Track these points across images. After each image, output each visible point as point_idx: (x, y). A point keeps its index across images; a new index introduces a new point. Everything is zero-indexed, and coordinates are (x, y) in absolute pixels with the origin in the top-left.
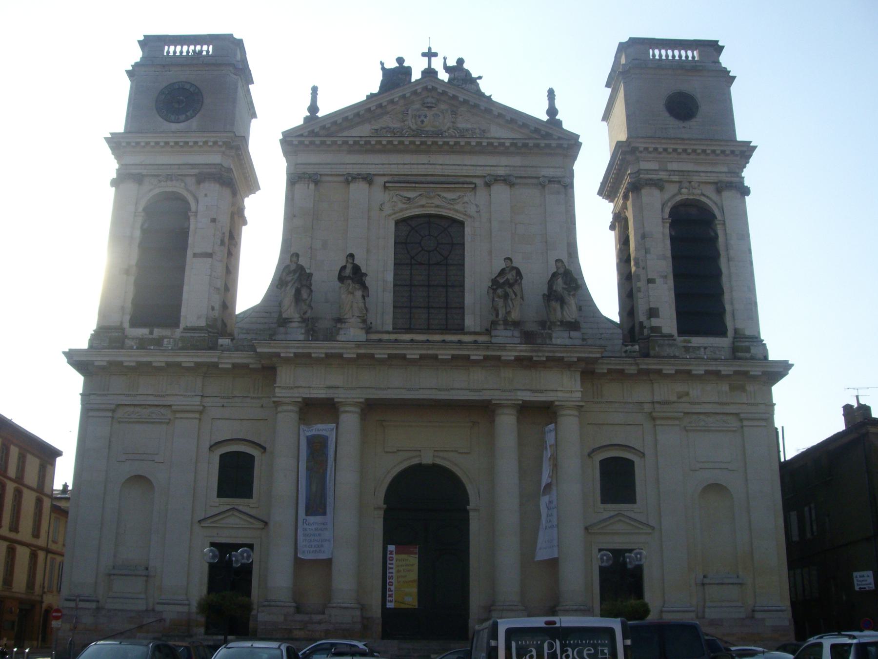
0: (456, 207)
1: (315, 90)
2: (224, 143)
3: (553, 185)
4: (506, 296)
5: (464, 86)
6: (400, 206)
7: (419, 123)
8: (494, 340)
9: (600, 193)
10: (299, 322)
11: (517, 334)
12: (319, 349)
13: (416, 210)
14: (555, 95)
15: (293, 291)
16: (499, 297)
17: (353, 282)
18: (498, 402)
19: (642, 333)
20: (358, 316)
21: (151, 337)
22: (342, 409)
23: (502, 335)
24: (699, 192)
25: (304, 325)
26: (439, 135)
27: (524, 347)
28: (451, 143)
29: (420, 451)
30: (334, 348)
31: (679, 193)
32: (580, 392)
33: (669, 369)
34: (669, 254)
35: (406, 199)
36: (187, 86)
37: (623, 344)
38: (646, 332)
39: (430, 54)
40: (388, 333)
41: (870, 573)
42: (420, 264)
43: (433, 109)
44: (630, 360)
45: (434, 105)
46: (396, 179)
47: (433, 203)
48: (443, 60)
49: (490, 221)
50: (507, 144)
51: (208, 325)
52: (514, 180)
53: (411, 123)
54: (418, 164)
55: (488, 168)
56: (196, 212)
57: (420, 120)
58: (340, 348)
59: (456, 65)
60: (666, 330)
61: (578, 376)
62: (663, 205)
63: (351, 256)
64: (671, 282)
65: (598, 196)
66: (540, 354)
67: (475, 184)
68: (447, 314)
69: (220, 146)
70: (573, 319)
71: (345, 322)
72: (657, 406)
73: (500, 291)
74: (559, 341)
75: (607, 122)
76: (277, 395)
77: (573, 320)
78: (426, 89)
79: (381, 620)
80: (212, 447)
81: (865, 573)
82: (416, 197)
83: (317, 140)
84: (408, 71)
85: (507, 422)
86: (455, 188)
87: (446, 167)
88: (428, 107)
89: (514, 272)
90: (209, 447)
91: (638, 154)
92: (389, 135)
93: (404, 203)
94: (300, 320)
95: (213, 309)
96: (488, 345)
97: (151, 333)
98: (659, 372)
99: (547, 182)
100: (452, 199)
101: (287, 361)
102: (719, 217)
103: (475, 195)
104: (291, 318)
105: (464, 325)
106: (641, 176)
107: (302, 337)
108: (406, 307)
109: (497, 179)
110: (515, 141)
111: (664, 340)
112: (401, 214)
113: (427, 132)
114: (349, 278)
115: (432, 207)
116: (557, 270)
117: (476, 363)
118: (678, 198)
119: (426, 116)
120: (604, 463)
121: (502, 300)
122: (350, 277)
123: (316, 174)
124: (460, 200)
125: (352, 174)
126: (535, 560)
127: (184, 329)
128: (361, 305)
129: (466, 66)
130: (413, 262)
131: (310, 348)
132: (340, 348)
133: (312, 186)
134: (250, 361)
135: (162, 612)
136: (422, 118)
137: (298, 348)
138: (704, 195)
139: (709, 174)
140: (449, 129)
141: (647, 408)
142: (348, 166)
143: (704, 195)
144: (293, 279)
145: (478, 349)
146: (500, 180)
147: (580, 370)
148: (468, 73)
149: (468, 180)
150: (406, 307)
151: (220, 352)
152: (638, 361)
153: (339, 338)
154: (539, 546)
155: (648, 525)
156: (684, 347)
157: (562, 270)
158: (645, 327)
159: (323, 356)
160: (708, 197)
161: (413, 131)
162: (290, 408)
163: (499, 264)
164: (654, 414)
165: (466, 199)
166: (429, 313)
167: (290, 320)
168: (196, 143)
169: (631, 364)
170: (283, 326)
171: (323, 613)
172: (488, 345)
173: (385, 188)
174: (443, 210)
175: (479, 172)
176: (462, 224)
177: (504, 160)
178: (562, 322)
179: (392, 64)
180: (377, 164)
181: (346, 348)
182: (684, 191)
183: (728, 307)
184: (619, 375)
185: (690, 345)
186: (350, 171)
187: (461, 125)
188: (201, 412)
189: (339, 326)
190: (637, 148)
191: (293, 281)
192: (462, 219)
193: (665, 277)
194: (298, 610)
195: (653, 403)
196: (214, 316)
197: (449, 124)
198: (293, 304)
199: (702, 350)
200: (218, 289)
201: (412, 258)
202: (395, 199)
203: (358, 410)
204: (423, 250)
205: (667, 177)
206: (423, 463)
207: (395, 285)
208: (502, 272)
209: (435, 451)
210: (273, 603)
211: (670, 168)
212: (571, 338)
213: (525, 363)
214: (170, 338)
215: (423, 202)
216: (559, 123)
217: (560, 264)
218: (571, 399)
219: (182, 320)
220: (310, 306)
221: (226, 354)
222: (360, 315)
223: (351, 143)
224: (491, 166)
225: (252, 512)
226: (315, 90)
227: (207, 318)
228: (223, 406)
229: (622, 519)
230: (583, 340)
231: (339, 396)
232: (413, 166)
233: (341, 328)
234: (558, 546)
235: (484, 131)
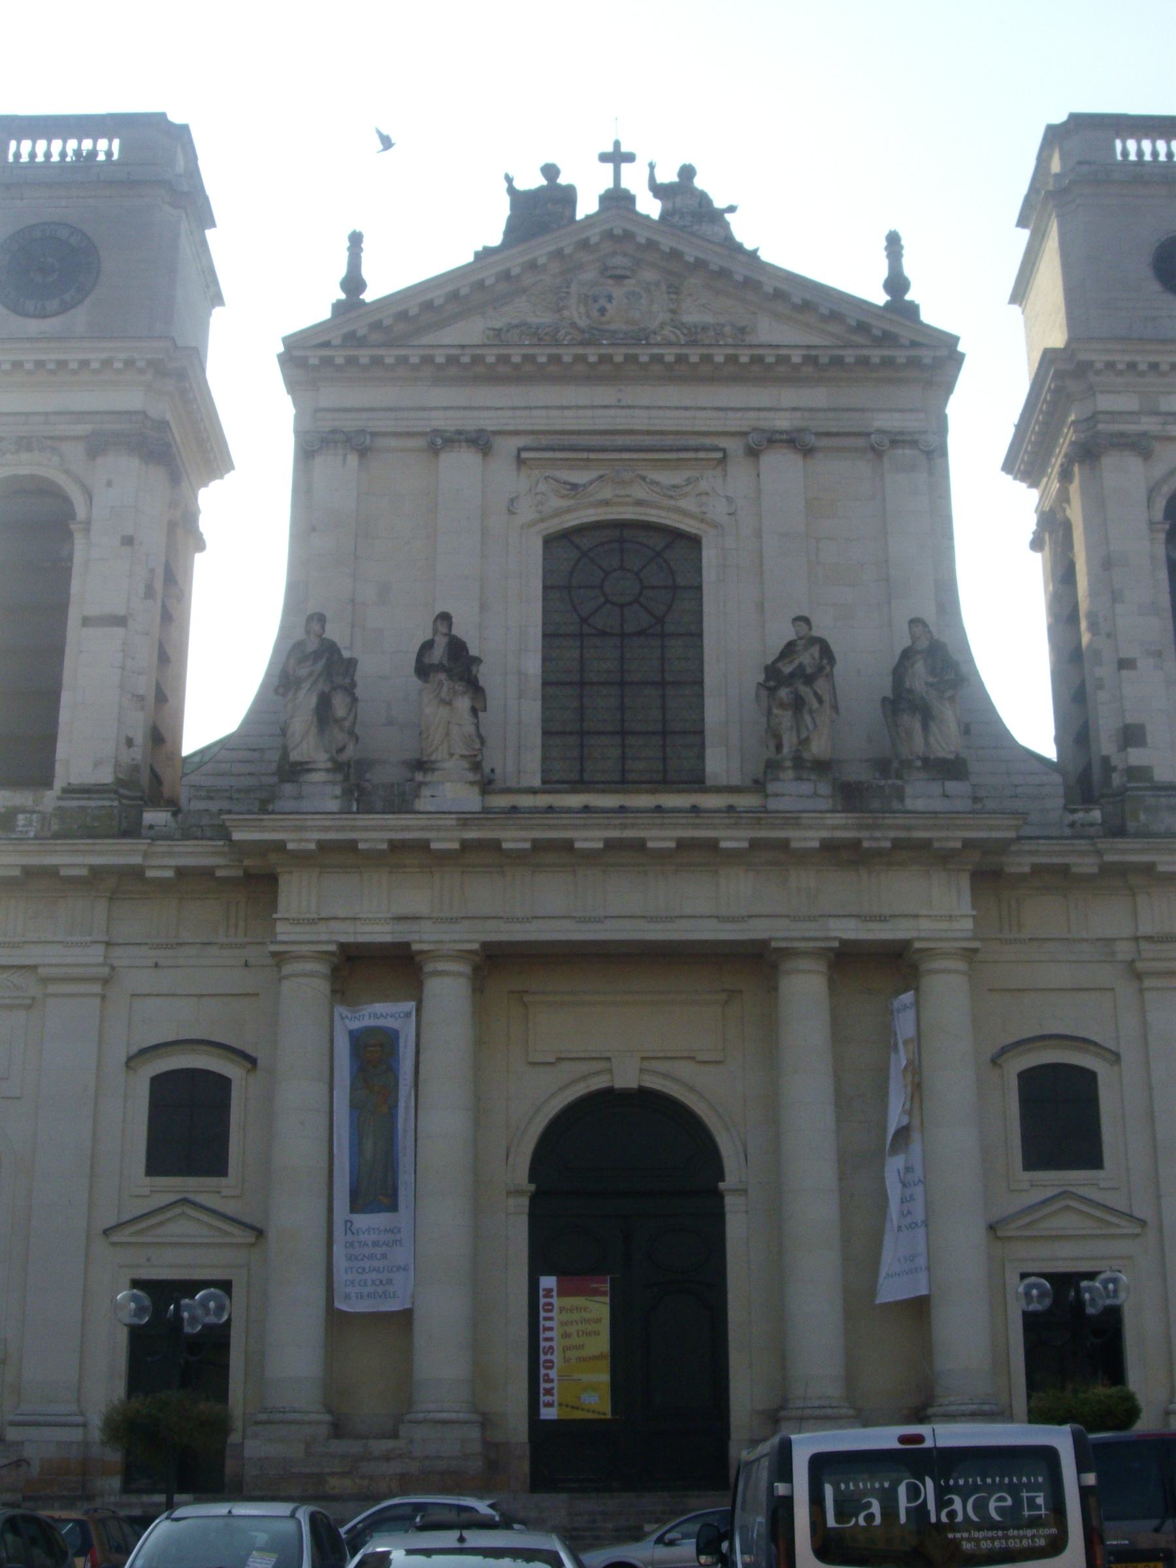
0: (682, 503)
1: (356, 240)
2: (150, 363)
3: (900, 451)
4: (798, 704)
5: (696, 228)
6: (556, 502)
7: (595, 314)
8: (772, 804)
9: (1009, 466)
10: (327, 770)
11: (824, 789)
13: (591, 511)
14: (902, 248)
15: (314, 700)
16: (782, 706)
17: (450, 678)
18: (783, 944)
19: (1107, 780)
20: (463, 756)
22: (429, 967)
25: (339, 777)
26: (641, 340)
27: (839, 819)
28: (670, 358)
29: (609, 1059)
30: (407, 828)
32: (970, 921)
35: (568, 487)
37: (1065, 808)
38: (1117, 779)
39: (617, 157)
40: (533, 791)
42: (603, 634)
43: (627, 282)
44: (1082, 845)
45: (628, 273)
46: (544, 441)
47: (627, 496)
48: (647, 170)
49: (759, 533)
50: (796, 359)
51: (120, 782)
52: (812, 440)
53: (576, 313)
54: (593, 407)
55: (752, 414)
56: (88, 523)
57: (597, 306)
58: (423, 828)
59: (676, 179)
61: (965, 882)
63: (445, 618)
65: (1003, 473)
66: (878, 834)
67: (724, 450)
68: (664, 746)
69: (141, 371)
70: (952, 752)
71: (433, 770)
72: (1143, 945)
73: (783, 693)
74: (920, 805)
75: (1020, 305)
76: (280, 938)
77: (952, 757)
78: (609, 235)
79: (527, 1447)
80: (132, 1061)
82: (591, 483)
83: (364, 356)
84: (567, 196)
86: (679, 460)
88: (611, 277)
89: (815, 650)
90: (124, 1059)
92: (527, 343)
93: (562, 497)
94: (329, 765)
95: (130, 742)
96: (759, 816)
98: (1148, 870)
99: (887, 442)
100: (674, 487)
101: (302, 859)
103: (725, 476)
104: (307, 763)
105: (703, 771)
106: (1101, 427)
107: (333, 805)
108: (571, 733)
109: (773, 439)
110: (813, 353)
111: (1159, 796)
112: (556, 521)
114: (440, 668)
115: (627, 504)
116: (913, 643)
117: (735, 857)
119: (610, 298)
120: (1028, 1078)
121: (789, 713)
122: (443, 665)
123: (362, 432)
124: (690, 487)
125: (445, 431)
126: (877, 1302)
128: (470, 729)
129: (699, 183)
130: (586, 630)
131: (354, 829)
132: (423, 828)
133: (353, 460)
134: (221, 861)
136: (603, 302)
137: (327, 829)
140: (662, 326)
141: (1124, 951)
142: (434, 414)
144: (311, 674)
145: (735, 824)
146: (781, 441)
147: (970, 867)
148: (703, 199)
149: (707, 441)
150: (571, 733)
151: (149, 841)
152: (1100, 846)
153: (420, 805)
154: (884, 1270)
155: (1130, 1217)
157: (924, 644)
158: (1114, 769)
159: (385, 846)
161: (582, 332)
162: (310, 966)
163: (782, 633)
164: (1139, 965)
165: (703, 485)
166: (623, 746)
167: (310, 766)
168: (84, 364)
169: (1083, 853)
170: (293, 782)
171: (395, 1435)
172: (759, 816)
173: (520, 462)
174: (653, 512)
175: (735, 422)
176: (695, 542)
177: (790, 396)
178: (925, 760)
179: (532, 180)
180: (501, 409)
181: (439, 829)
187: (692, 316)
188: (106, 981)
189: (419, 777)
190: (1090, 364)
191: (312, 679)
192: (693, 531)
193: (1159, 654)
194: (338, 1429)
195: (1136, 939)
196: (133, 759)
198: (314, 730)
200: (141, 698)
201: (584, 620)
202: (542, 487)
203: (465, 968)
204: (607, 601)
205: (1159, 427)
207: (545, 684)
208: (789, 650)
209: (643, 1058)
212: (947, 796)
214: (33, 812)
215: (607, 493)
216: (912, 310)
217: (918, 630)
218: (950, 935)
219: (59, 769)
220: (352, 733)
221: (161, 846)
222: (467, 753)
223: (440, 360)
224: (760, 409)
225: (230, 1208)
226: (356, 240)
227: (117, 765)
228: (156, 965)
229: (1072, 1203)
230: (976, 799)
231: (422, 937)
232: (581, 413)
233: (425, 784)
234: (928, 1269)
235: (742, 330)
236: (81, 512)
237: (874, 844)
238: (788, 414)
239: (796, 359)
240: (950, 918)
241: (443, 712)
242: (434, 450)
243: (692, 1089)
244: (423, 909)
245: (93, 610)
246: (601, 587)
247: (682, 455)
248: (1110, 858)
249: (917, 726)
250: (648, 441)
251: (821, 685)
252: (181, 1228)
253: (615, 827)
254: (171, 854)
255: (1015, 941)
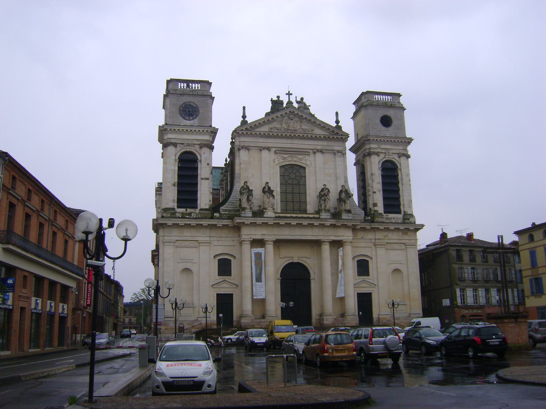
4: (325, 200)
6: (281, 160)
7: (288, 126)
8: (321, 217)
11: (329, 214)
12: (259, 221)
15: (246, 197)
16: (322, 200)
17: (269, 194)
21: (186, 212)
23: (324, 215)
24: (392, 157)
31: (385, 157)
33: (382, 227)
34: (381, 181)
36: (192, 104)
38: (372, 212)
39: (289, 94)
41: (448, 300)
42: (289, 184)
49: (315, 167)
52: (324, 151)
53: (284, 126)
60: (379, 212)
61: (351, 230)
62: (379, 162)
63: (267, 183)
64: (381, 193)
72: (376, 240)
73: (323, 198)
76: (243, 238)
80: (215, 257)
81: (447, 300)
84: (282, 103)
85: (326, 248)
87: (298, 145)
89: (327, 190)
91: (370, 142)
94: (249, 208)
97: (186, 211)
98: (378, 228)
101: (247, 225)
102: (399, 167)
105: (306, 208)
107: (251, 215)
109: (318, 151)
113: (291, 130)
114: (267, 192)
115: (293, 161)
118: (385, 159)
119: (290, 123)
127: (200, 210)
129: (304, 101)
130: (287, 183)
133: (247, 151)
134: (230, 223)
135: (201, 321)
136: (289, 124)
137: (252, 220)
138: (394, 158)
139: (396, 150)
141: (373, 241)
142: (261, 143)
143: (394, 158)
148: (305, 104)
149: (307, 150)
153: (265, 216)
154: (337, 292)
156: (386, 218)
157: (344, 190)
160: (395, 159)
161: (286, 129)
163: (321, 187)
164: (376, 244)
165: (306, 158)
169: (369, 225)
175: (311, 147)
176: (305, 168)
177: (320, 143)
179: (275, 99)
182: (387, 156)
183: (402, 203)
184: (364, 229)
185: (388, 217)
186: (261, 145)
187: (304, 127)
190: (370, 139)
193: (380, 191)
195: (375, 239)
196: (174, 185)
197: (299, 127)
198: (246, 202)
199: (392, 219)
201: (286, 182)
202: (279, 158)
206: (294, 262)
210: (247, 316)
211: (382, 148)
213: (333, 226)
215: (290, 159)
231: (266, 238)
233: (266, 212)
235: (312, 130)
236: (199, 158)
237: (338, 225)
238: (320, 146)
239: (322, 137)
240: (349, 236)
241: (268, 200)
242: (261, 150)
243: (306, 262)
244: (266, 233)
245: (203, 177)
246: (289, 176)
247: (303, 153)
248: (373, 226)
249: (344, 204)
250: (296, 150)
251: (328, 196)
252: (225, 285)
253: (298, 221)
254: (222, 222)
255: (356, 239)
